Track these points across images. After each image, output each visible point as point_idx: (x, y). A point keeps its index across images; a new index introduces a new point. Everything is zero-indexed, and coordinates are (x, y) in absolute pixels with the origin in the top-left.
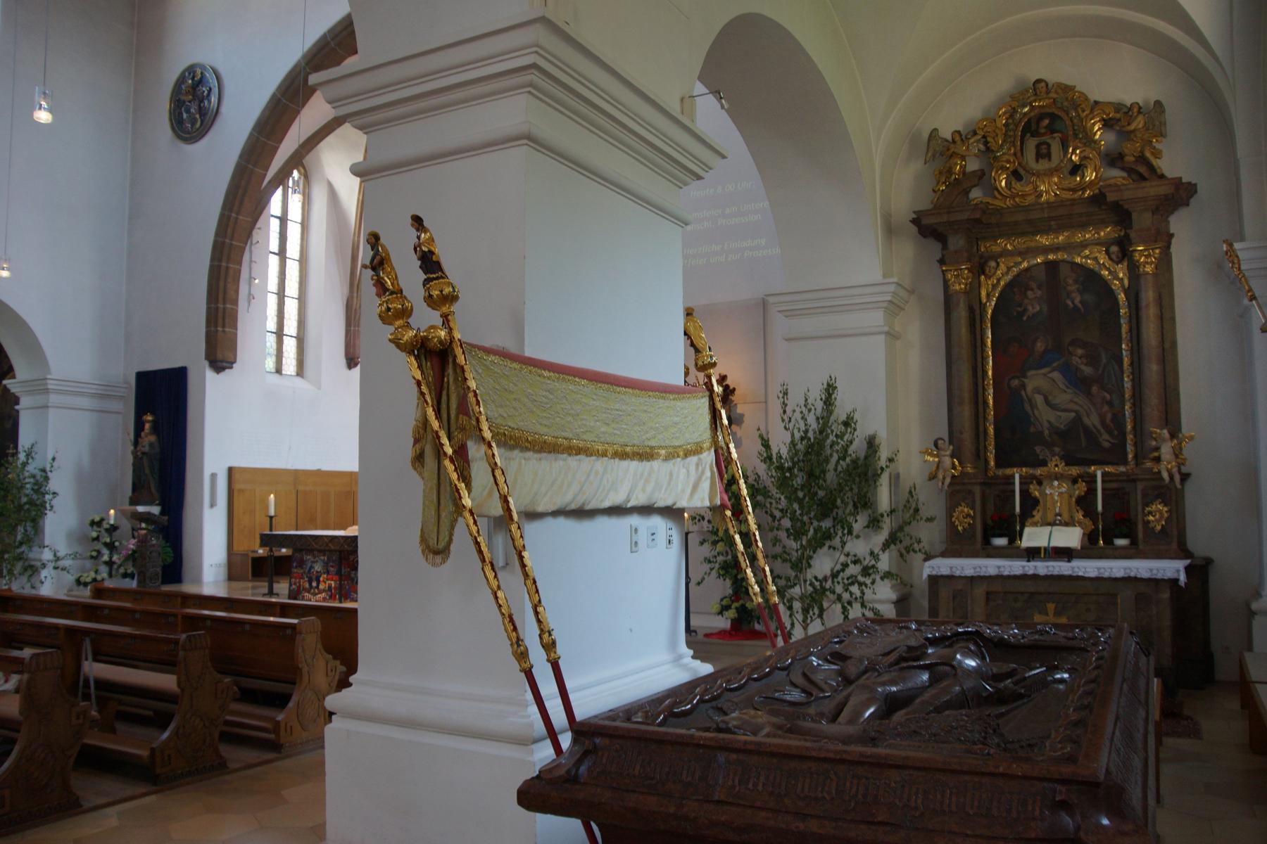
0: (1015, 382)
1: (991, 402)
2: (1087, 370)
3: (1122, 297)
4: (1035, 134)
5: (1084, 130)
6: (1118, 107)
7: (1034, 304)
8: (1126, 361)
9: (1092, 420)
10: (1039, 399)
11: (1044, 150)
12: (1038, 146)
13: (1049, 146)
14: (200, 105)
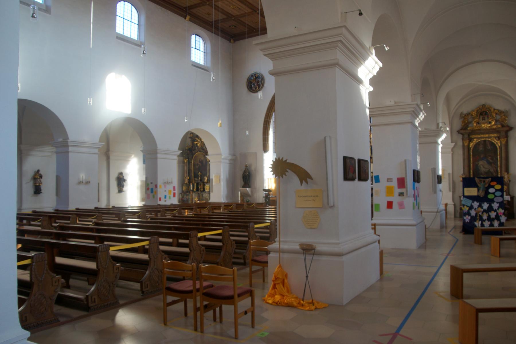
0: (477, 163)
1: (472, 166)
2: (491, 161)
3: (498, 148)
4: (482, 115)
5: (492, 115)
6: (498, 110)
7: (481, 148)
8: (499, 160)
9: (492, 170)
10: (482, 166)
11: (484, 118)
12: (483, 118)
13: (485, 118)
14: (258, 84)
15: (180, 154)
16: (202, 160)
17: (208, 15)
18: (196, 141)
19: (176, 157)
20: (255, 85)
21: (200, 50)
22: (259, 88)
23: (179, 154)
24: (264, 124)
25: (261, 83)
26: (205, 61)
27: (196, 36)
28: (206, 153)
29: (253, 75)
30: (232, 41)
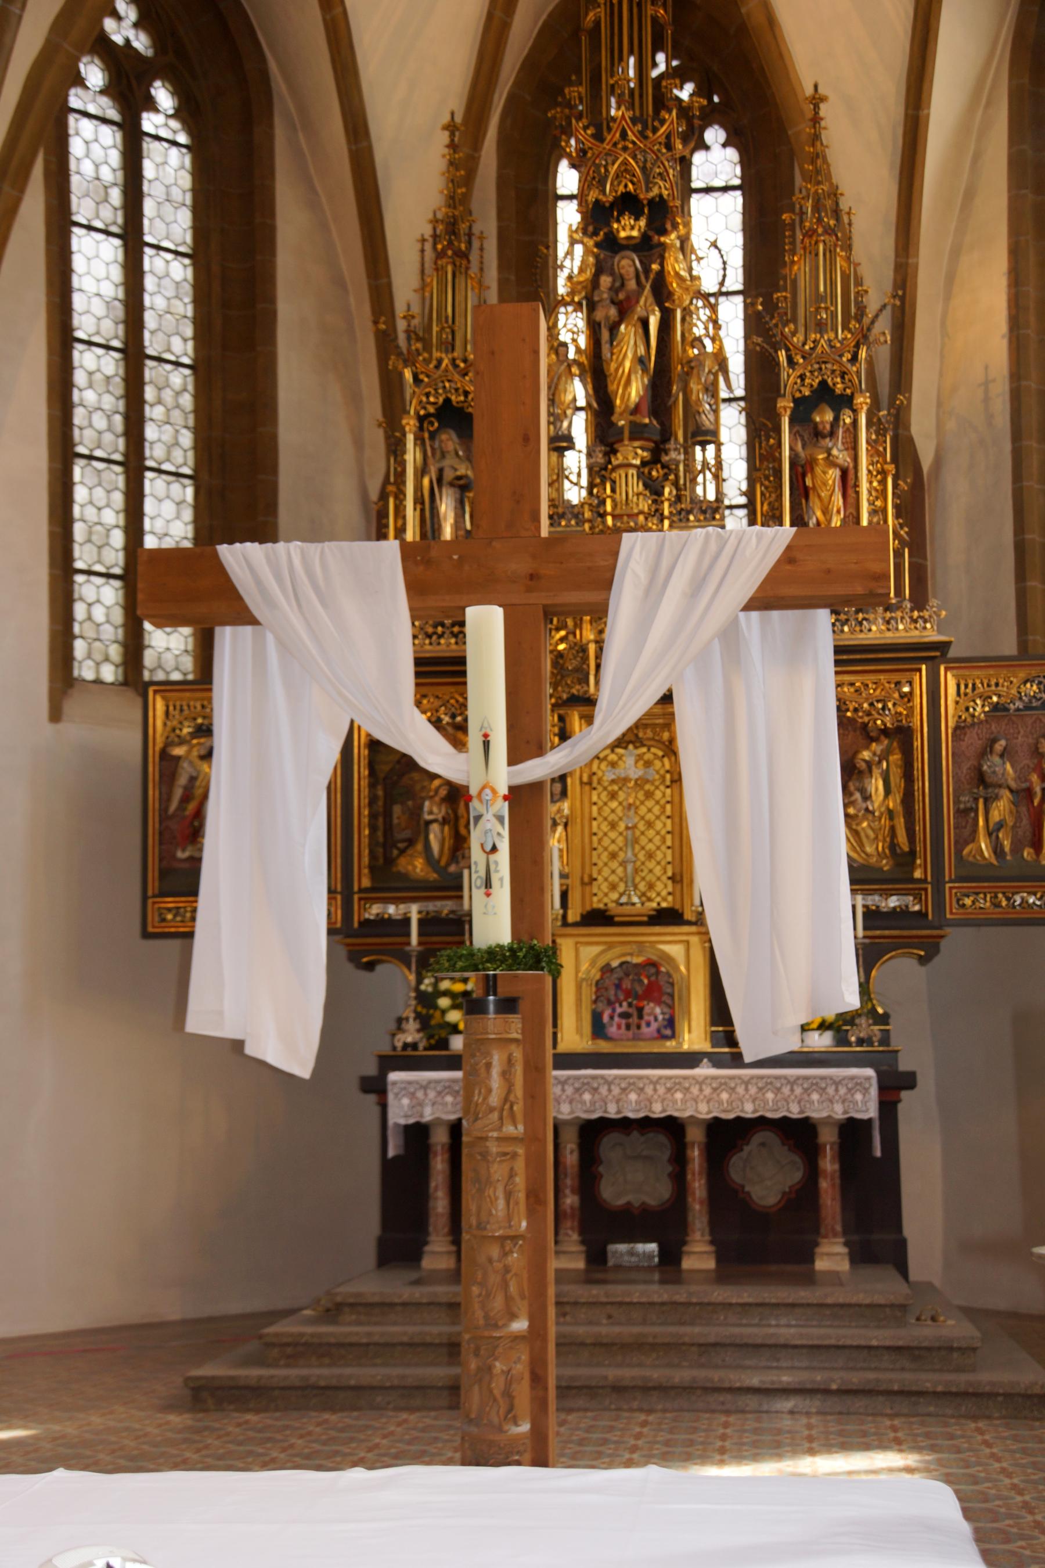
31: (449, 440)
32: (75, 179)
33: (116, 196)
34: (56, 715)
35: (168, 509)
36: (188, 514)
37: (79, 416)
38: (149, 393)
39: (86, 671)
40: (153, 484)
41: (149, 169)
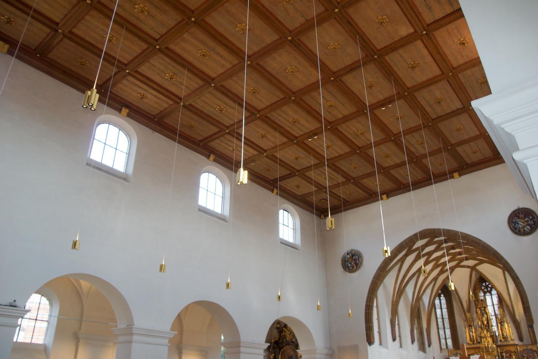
14: (355, 262)
15: (267, 348)
16: (290, 355)
17: (298, 187)
18: (283, 332)
19: (262, 352)
20: (352, 263)
21: (288, 226)
22: (356, 268)
23: (266, 348)
24: (366, 310)
25: (359, 261)
26: (295, 238)
27: (284, 211)
28: (297, 346)
29: (349, 253)
30: (323, 216)
31: (470, 327)
32: (436, 305)
33: (439, 305)
34: (441, 352)
35: (448, 332)
36: (450, 332)
37: (439, 325)
38: (445, 322)
39: (443, 347)
40: (446, 330)
41: (442, 302)
